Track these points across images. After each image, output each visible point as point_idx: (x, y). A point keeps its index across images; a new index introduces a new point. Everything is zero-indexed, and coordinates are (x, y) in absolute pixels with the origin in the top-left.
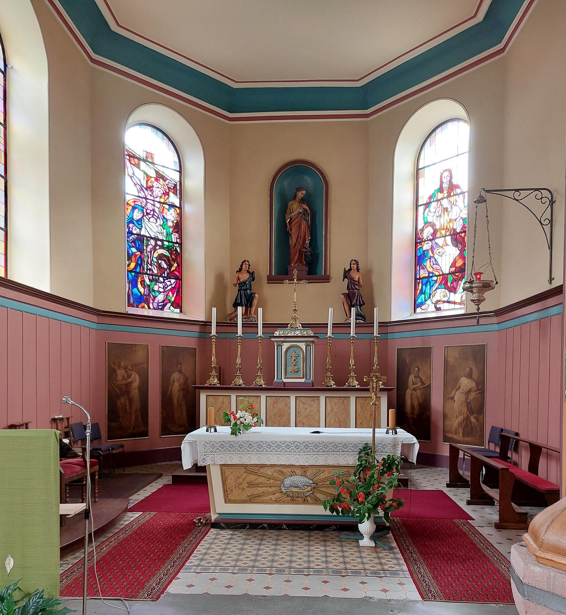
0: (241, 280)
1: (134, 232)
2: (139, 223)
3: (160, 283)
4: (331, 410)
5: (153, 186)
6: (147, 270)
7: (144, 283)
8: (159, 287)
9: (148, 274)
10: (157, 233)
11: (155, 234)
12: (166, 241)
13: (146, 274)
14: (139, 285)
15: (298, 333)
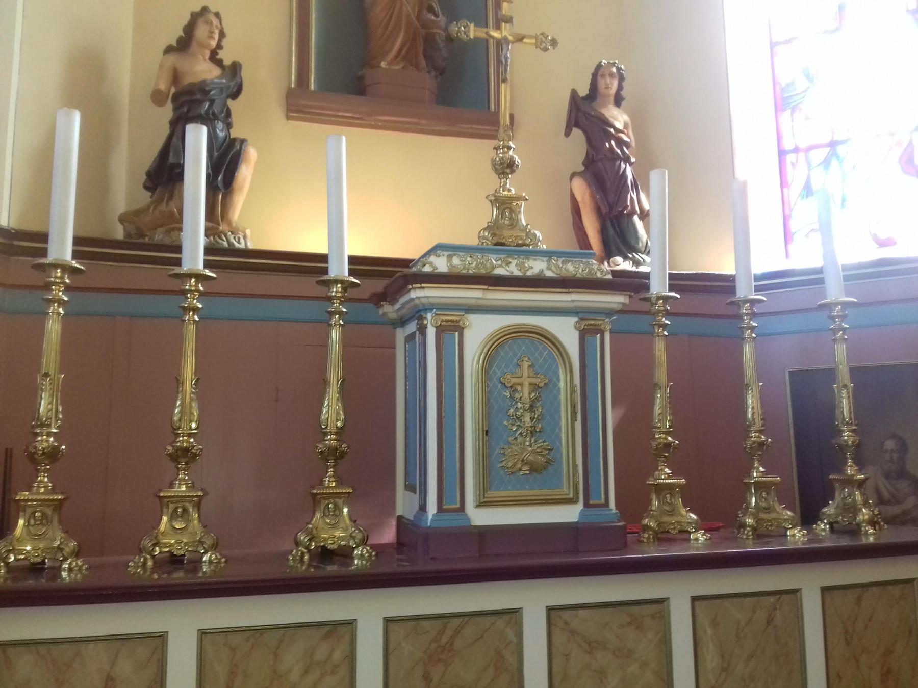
0: (188, 80)
4: (724, 670)
15: (537, 267)
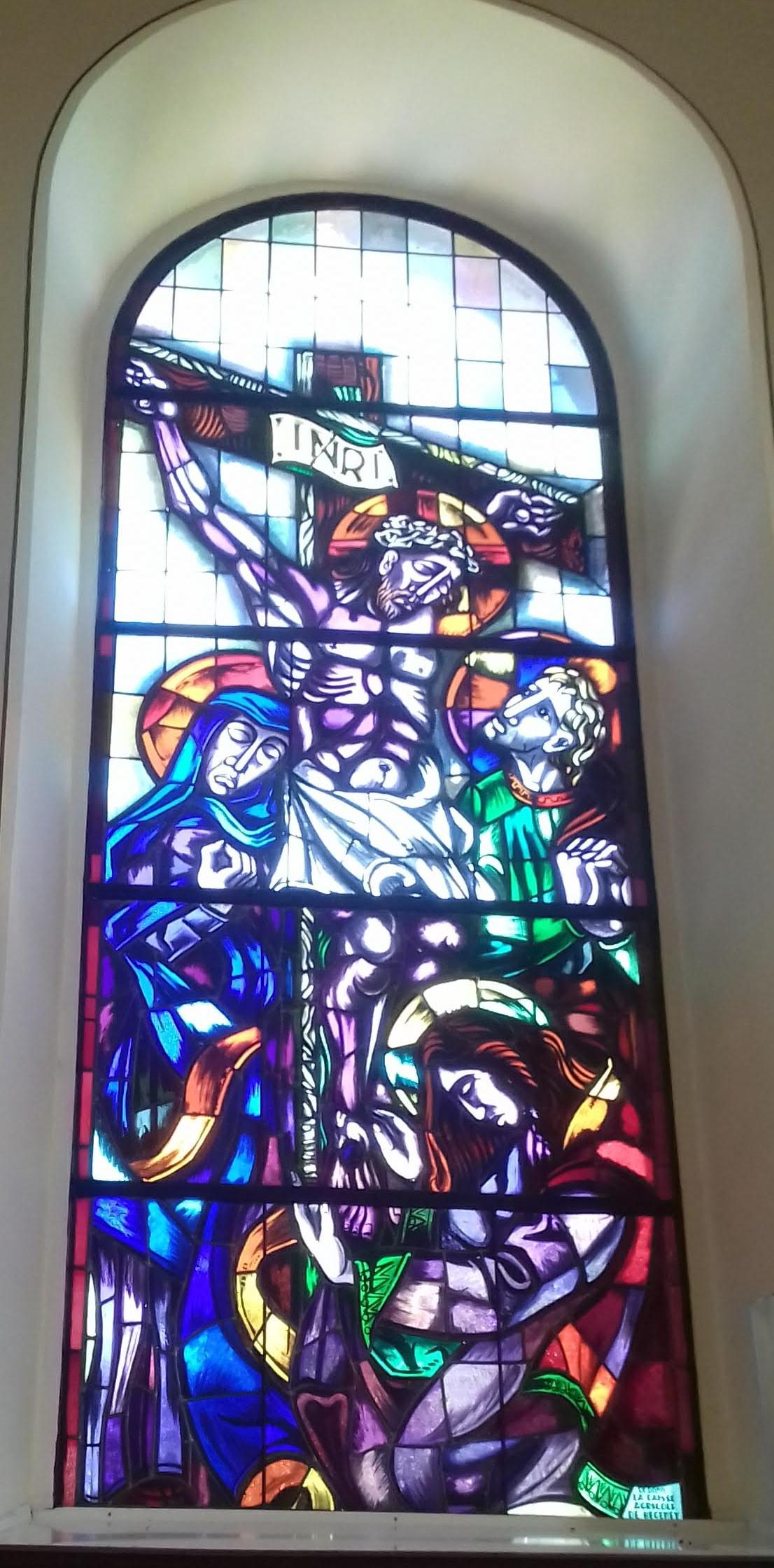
1: (209, 879)
2: (259, 811)
3: (461, 1260)
5: (376, 551)
6: (325, 1160)
7: (298, 1279)
8: (450, 1297)
9: (337, 1198)
10: (420, 865)
11: (392, 870)
12: (503, 907)
13: (319, 1191)
14: (250, 1299)
